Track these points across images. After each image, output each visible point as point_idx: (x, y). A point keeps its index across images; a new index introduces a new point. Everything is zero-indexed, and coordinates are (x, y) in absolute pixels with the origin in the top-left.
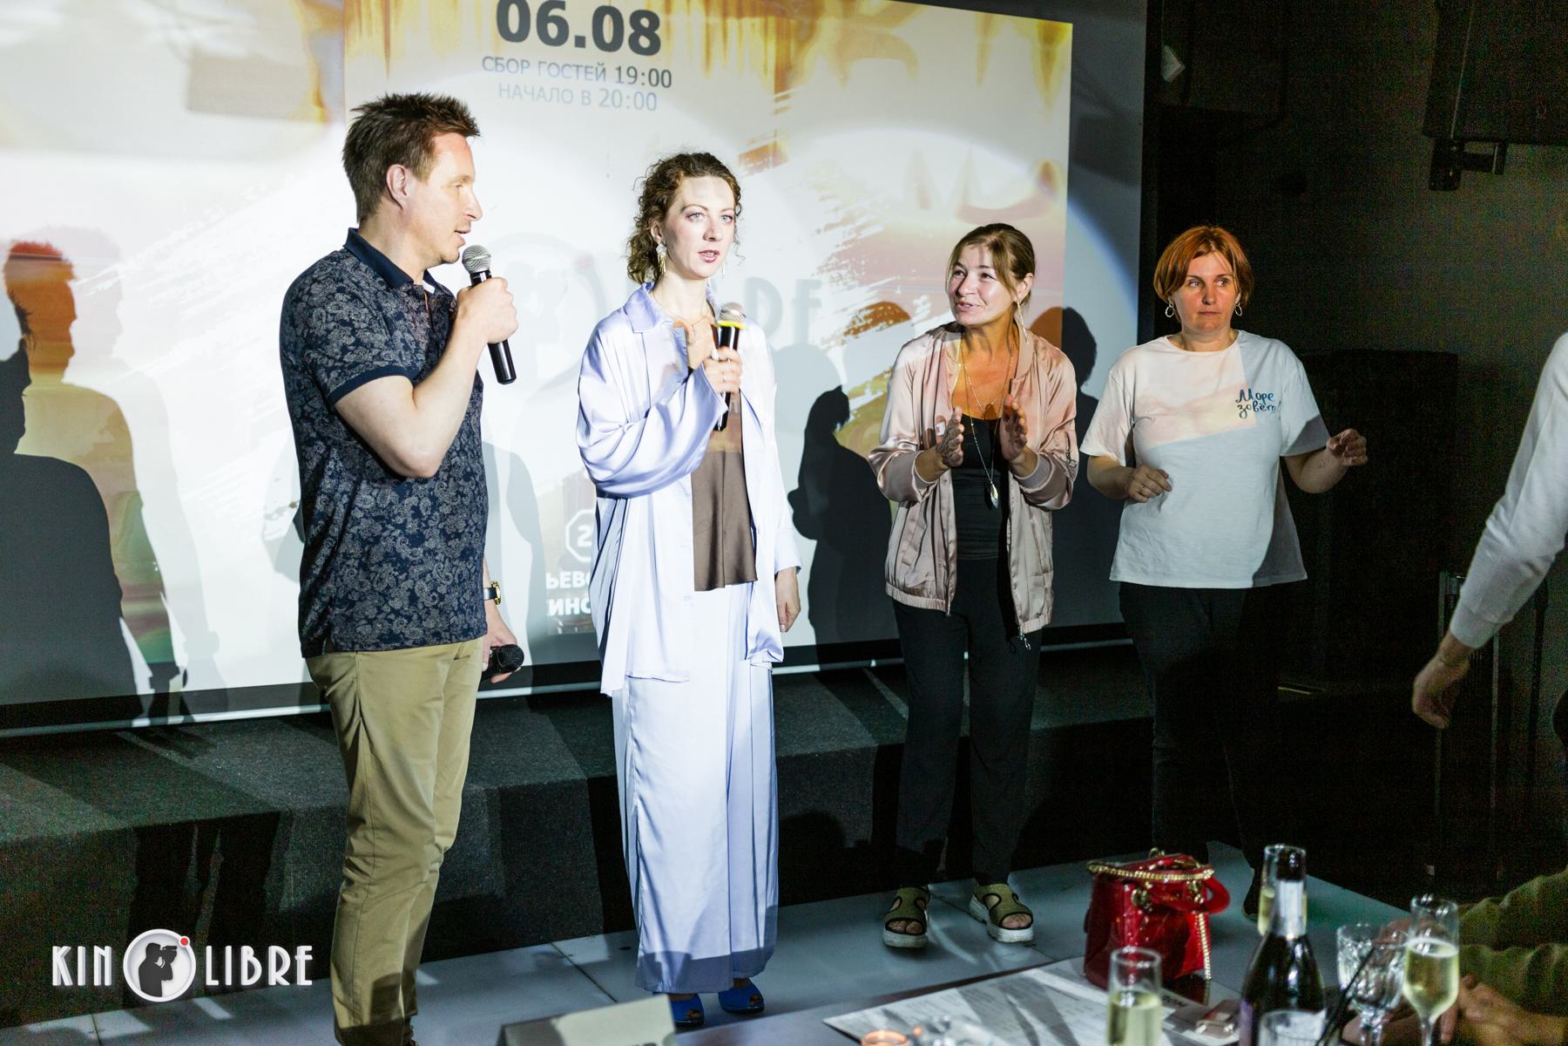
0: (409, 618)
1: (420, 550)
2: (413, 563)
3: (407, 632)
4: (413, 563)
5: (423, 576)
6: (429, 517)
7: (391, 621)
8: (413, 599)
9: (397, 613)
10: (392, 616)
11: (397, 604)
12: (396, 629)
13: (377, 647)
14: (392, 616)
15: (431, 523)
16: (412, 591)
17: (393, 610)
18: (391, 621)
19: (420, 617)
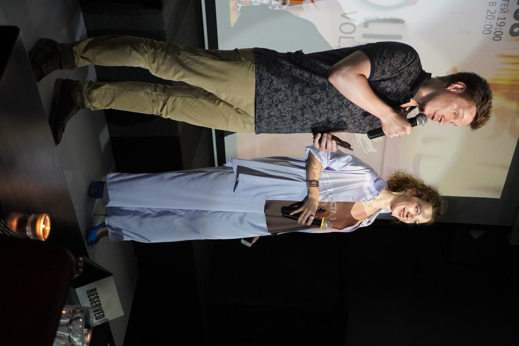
0: (268, 88)
1: (297, 94)
2: (292, 91)
3: (262, 87)
4: (292, 91)
5: (286, 95)
6: (311, 98)
7: (268, 79)
8: (277, 90)
9: (271, 82)
10: (270, 80)
11: (275, 82)
12: (265, 82)
13: (257, 74)
14: (270, 80)
15: (309, 99)
16: (280, 90)
17: (273, 80)
18: (268, 79)
19: (269, 94)
